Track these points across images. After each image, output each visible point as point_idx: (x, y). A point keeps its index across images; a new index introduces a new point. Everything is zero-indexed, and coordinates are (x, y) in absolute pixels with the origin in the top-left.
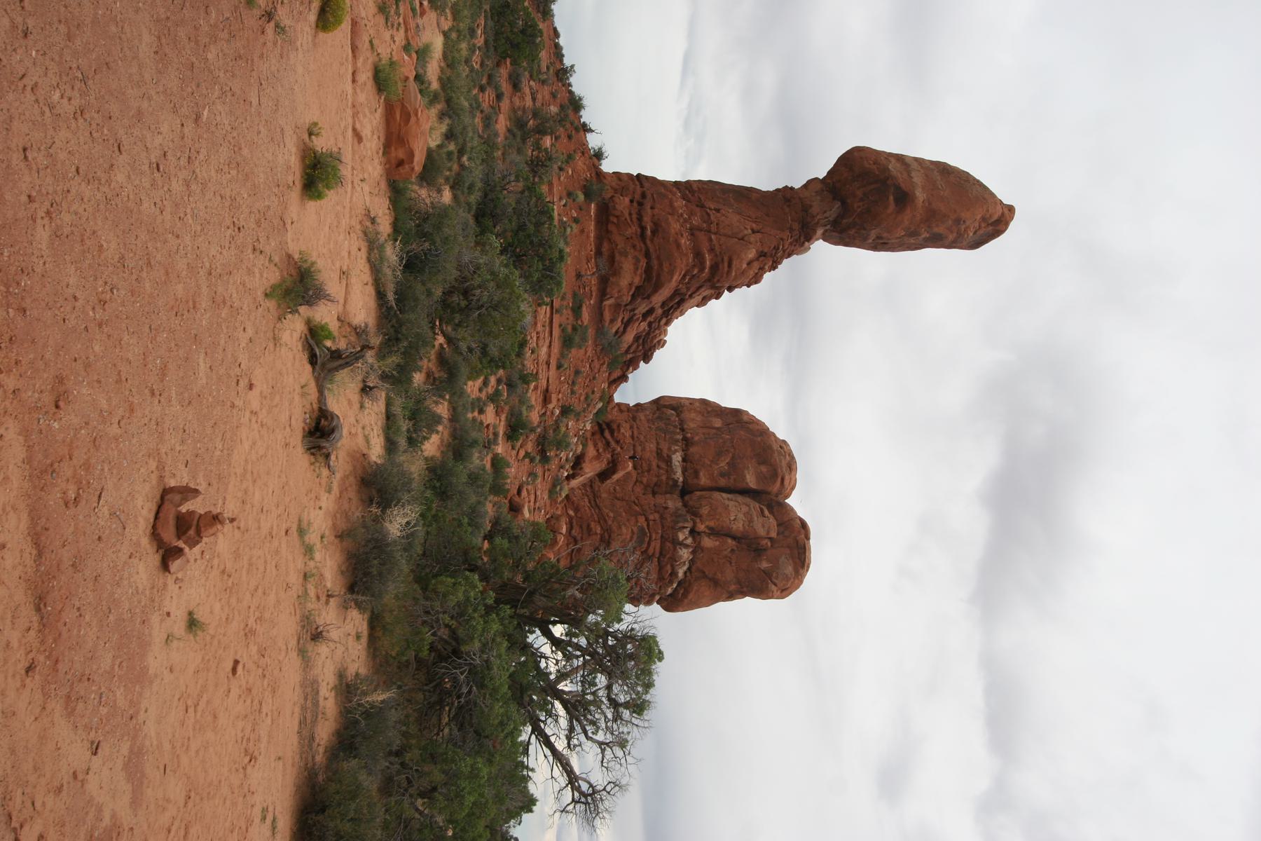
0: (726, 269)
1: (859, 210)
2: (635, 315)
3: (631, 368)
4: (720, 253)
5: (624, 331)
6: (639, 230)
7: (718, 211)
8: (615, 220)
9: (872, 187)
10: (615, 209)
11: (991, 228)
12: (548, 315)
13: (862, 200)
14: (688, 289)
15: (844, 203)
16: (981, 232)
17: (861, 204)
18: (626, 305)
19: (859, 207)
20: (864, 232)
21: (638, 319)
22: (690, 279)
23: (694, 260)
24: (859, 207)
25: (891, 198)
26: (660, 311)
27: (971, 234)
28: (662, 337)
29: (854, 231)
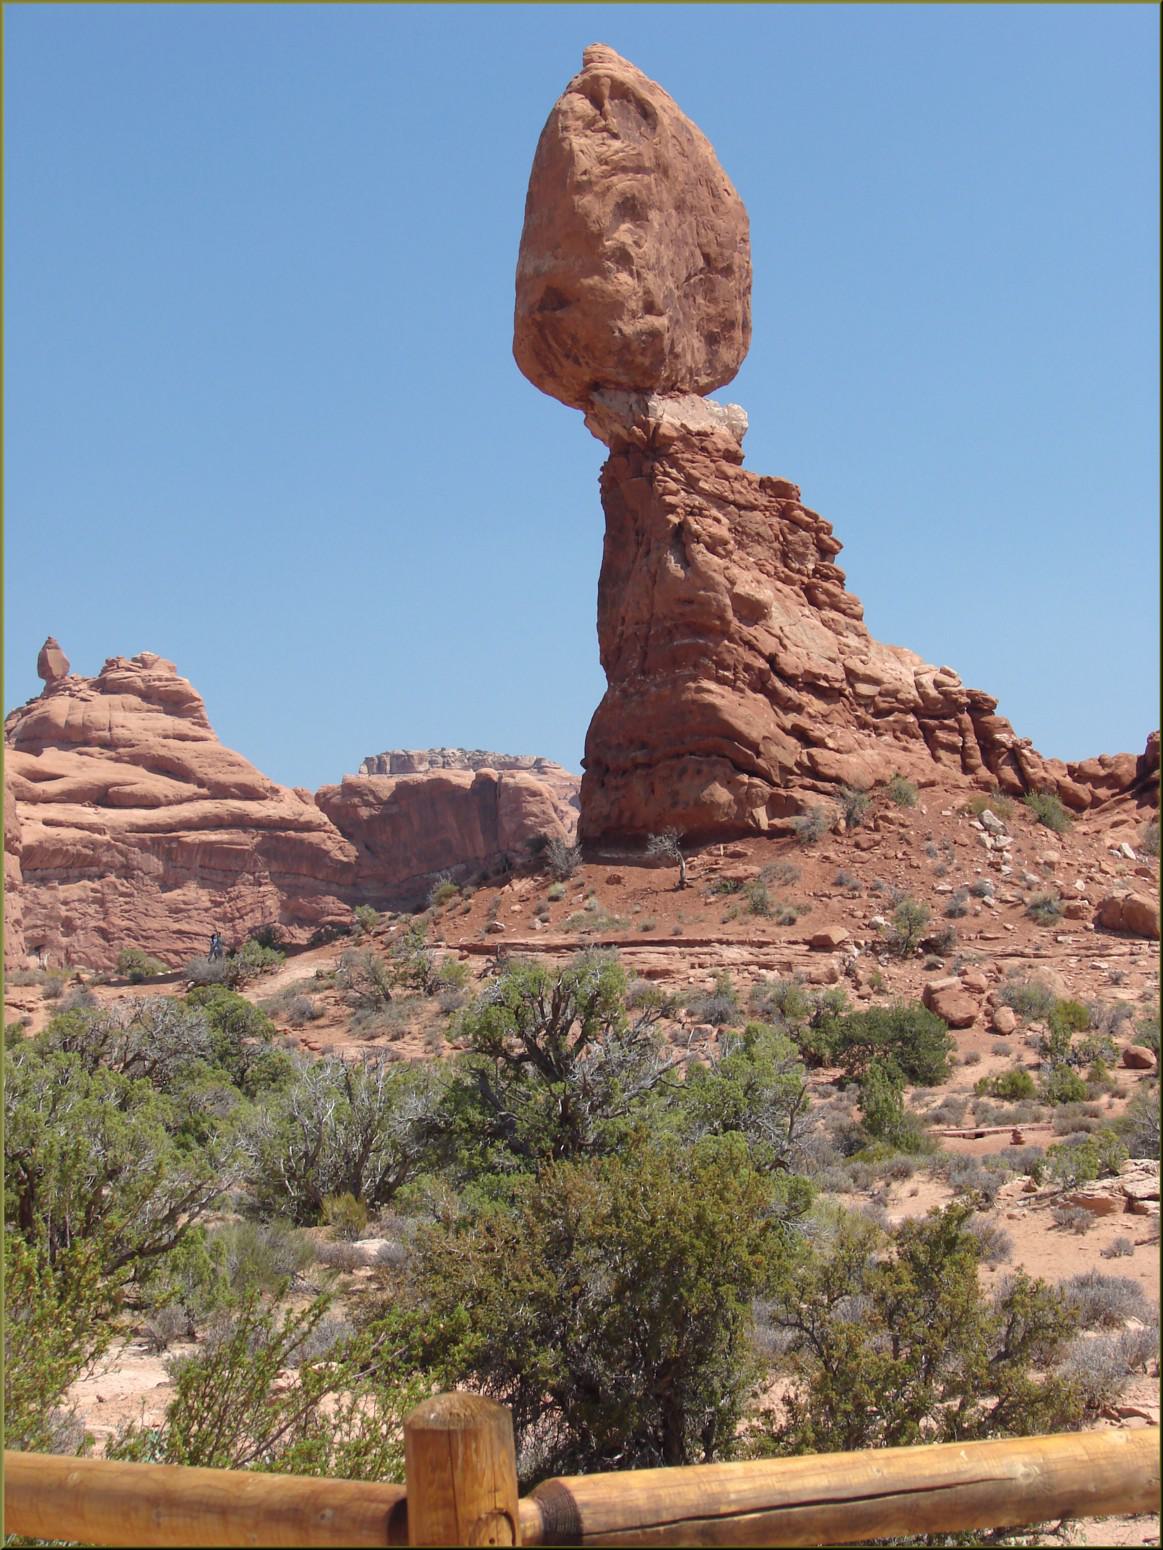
0: (695, 607)
1: (592, 364)
2: (799, 764)
3: (1001, 737)
4: (672, 619)
5: (837, 780)
6: (639, 771)
7: (623, 619)
8: (627, 814)
9: (553, 343)
10: (608, 817)
11: (608, 105)
12: (674, 949)
13: (576, 361)
14: (748, 668)
15: (596, 386)
16: (614, 123)
17: (581, 360)
18: (773, 784)
19: (587, 363)
20: (635, 345)
21: (810, 757)
22: (727, 668)
23: (685, 667)
24: (587, 363)
25: (559, 314)
26: (816, 705)
27: (617, 144)
28: (927, 680)
29: (639, 359)
